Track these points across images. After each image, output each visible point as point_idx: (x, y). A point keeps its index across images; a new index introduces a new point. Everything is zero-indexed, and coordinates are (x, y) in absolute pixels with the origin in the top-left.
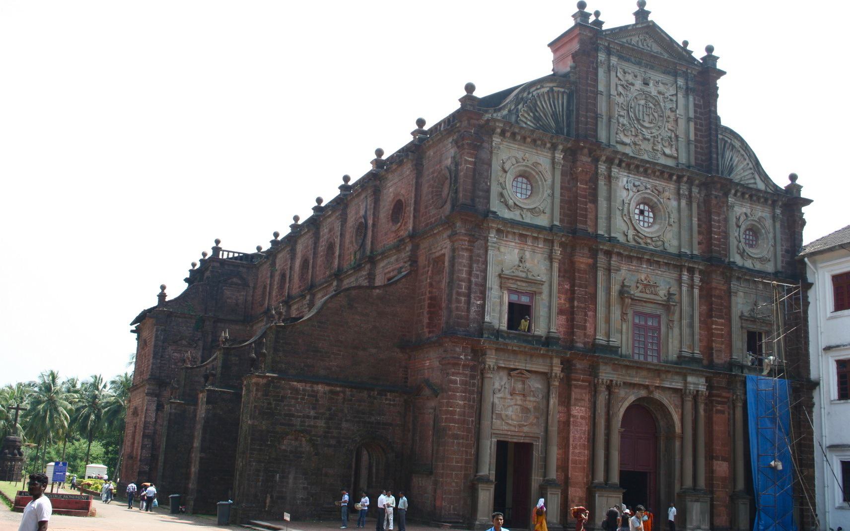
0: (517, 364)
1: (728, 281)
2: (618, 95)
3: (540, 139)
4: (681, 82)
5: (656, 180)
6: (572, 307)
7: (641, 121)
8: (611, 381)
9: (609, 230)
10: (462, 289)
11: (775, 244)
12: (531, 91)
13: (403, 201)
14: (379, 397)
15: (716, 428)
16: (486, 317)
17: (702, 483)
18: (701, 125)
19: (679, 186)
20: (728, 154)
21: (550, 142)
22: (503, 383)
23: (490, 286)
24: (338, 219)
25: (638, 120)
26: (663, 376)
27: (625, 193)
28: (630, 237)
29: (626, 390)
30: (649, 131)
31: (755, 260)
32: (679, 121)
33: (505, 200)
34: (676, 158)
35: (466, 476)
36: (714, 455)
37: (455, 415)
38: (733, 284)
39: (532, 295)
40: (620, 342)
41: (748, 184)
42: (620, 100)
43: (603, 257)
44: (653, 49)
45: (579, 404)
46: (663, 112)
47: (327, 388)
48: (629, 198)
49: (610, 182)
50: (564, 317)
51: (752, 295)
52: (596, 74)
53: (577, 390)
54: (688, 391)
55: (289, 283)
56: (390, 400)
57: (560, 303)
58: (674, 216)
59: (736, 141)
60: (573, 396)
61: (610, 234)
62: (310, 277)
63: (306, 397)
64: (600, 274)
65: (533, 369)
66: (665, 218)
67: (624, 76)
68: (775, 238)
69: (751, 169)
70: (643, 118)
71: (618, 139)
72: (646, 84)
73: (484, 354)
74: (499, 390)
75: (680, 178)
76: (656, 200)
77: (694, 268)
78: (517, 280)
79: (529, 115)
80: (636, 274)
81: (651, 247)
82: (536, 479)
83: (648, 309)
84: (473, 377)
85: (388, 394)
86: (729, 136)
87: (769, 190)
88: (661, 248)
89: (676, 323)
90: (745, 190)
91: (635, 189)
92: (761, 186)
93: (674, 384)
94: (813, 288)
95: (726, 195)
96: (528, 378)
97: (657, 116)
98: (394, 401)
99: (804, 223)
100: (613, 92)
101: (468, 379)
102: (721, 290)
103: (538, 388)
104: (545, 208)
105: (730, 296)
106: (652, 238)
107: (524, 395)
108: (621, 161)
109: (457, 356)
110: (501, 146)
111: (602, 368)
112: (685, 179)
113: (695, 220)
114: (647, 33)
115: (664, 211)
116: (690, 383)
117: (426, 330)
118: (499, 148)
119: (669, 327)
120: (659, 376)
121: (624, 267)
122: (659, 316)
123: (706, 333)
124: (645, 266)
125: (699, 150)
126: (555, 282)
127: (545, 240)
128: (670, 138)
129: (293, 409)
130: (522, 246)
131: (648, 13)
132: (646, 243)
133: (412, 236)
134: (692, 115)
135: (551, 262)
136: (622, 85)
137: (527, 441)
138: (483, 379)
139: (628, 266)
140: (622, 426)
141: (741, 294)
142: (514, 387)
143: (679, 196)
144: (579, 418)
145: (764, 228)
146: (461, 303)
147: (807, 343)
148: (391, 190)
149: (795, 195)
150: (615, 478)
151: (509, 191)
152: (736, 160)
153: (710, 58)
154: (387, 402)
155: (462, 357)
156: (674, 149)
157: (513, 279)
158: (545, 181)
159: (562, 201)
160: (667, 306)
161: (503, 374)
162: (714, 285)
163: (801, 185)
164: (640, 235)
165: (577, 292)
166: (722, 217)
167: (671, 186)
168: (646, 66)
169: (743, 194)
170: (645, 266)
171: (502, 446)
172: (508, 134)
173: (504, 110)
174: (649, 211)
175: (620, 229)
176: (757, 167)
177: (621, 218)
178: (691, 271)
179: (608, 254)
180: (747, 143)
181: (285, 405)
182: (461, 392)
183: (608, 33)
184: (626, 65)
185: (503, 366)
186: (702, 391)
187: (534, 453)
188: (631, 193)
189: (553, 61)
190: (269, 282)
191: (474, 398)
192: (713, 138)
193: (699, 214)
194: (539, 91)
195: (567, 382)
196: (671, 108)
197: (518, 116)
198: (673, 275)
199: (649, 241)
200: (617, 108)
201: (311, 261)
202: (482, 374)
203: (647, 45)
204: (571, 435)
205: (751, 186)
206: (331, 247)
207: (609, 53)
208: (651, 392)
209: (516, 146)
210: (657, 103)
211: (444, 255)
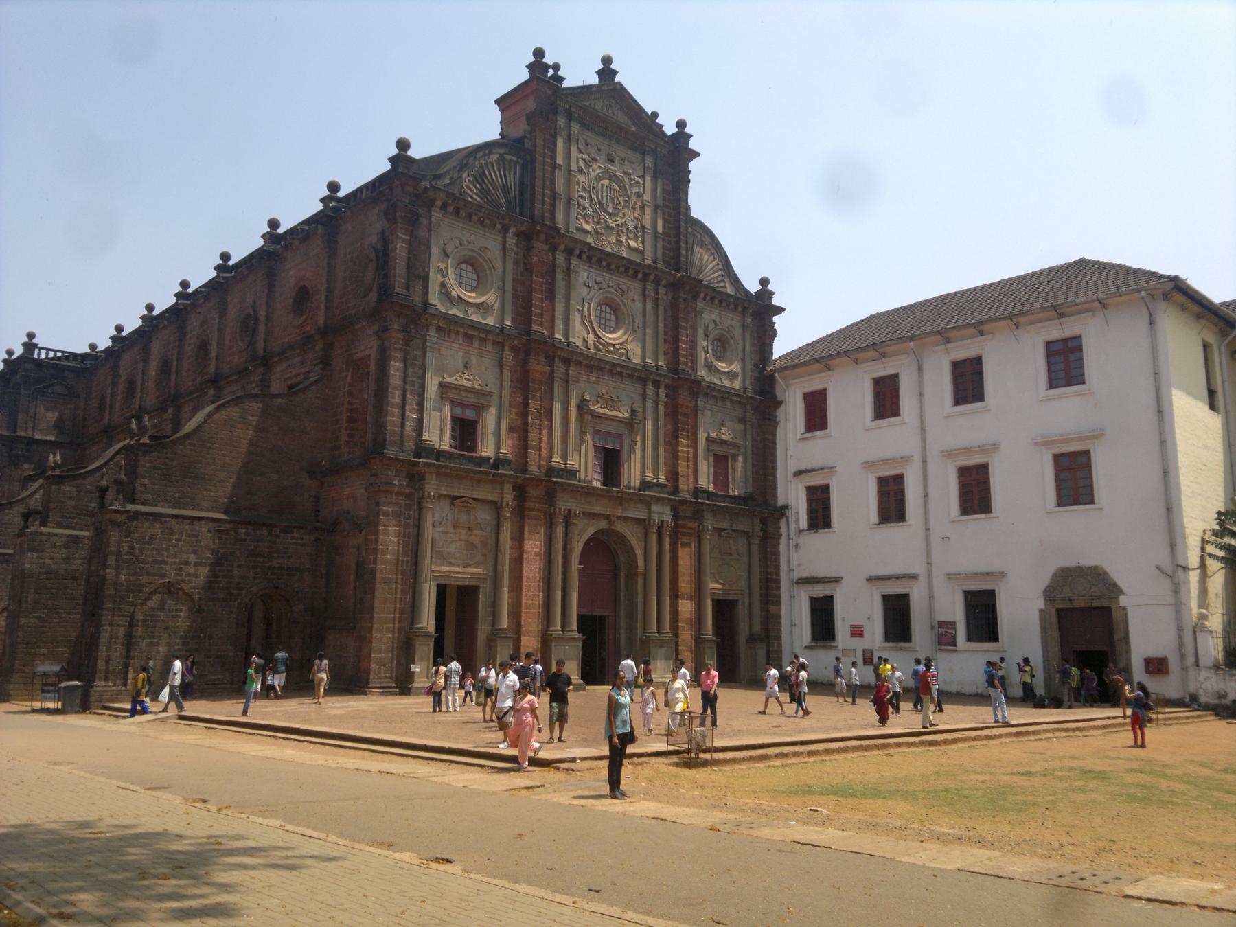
1: (695, 396)
4: (649, 162)
6: (526, 423)
7: (604, 206)
8: (570, 510)
9: (567, 334)
10: (394, 398)
12: (478, 155)
13: (309, 287)
14: (282, 534)
15: (681, 562)
16: (424, 434)
18: (670, 215)
19: (645, 285)
20: (698, 252)
22: (444, 514)
23: (429, 396)
24: (215, 309)
25: (601, 204)
27: (585, 288)
28: (590, 343)
33: (447, 291)
34: (642, 253)
35: (400, 629)
39: (480, 408)
40: (578, 464)
41: (718, 287)
43: (560, 365)
46: (628, 197)
47: (212, 525)
48: (590, 296)
49: (569, 276)
52: (555, 145)
54: (652, 521)
55: (141, 391)
56: (297, 539)
58: (639, 319)
61: (567, 338)
62: (173, 384)
63: (184, 537)
65: (480, 497)
67: (586, 149)
68: (744, 349)
69: (720, 270)
72: (611, 160)
73: (422, 478)
74: (440, 523)
75: (646, 276)
76: (619, 301)
77: (659, 381)
78: (461, 390)
79: (475, 187)
82: (482, 630)
83: (609, 427)
84: (408, 507)
85: (295, 531)
88: (624, 358)
89: (639, 444)
91: (596, 286)
92: (730, 290)
94: (783, 405)
95: (695, 298)
96: (473, 508)
97: (622, 201)
98: (302, 539)
99: (775, 334)
100: (574, 167)
101: (403, 510)
105: (696, 415)
107: (469, 529)
108: (581, 252)
110: (441, 223)
111: (559, 496)
112: (652, 278)
113: (661, 325)
116: (654, 513)
117: (344, 450)
118: (440, 225)
119: (632, 449)
122: (620, 436)
124: (606, 378)
125: (666, 244)
127: (495, 342)
129: (166, 554)
131: (615, 73)
132: (608, 352)
133: (324, 332)
134: (660, 202)
136: (584, 160)
137: (473, 583)
138: (420, 509)
140: (580, 564)
141: (708, 413)
143: (644, 295)
144: (533, 553)
146: (393, 416)
147: (774, 468)
148: (291, 273)
149: (766, 303)
150: (574, 625)
151: (451, 281)
152: (706, 258)
153: (682, 135)
154: (294, 541)
155: (396, 482)
156: (639, 242)
158: (495, 270)
159: (515, 296)
161: (445, 504)
162: (680, 401)
163: (773, 290)
165: (531, 406)
166: (690, 324)
169: (712, 299)
170: (606, 378)
171: (442, 590)
172: (450, 209)
174: (611, 314)
175: (580, 335)
177: (580, 320)
178: (656, 384)
179: (567, 361)
180: (717, 240)
181: (154, 549)
182: (394, 526)
183: (568, 91)
184: (588, 135)
185: (445, 493)
186: (668, 522)
187: (481, 596)
188: (592, 292)
189: (501, 122)
190: (109, 391)
191: (409, 533)
192: (682, 230)
193: (665, 320)
195: (520, 512)
196: (637, 193)
198: (639, 389)
200: (577, 187)
201: (175, 363)
202: (420, 503)
203: (613, 113)
204: (525, 574)
205: (720, 290)
206: (204, 346)
207: (570, 117)
208: (611, 523)
209: (461, 225)
210: (623, 187)
211: (369, 356)
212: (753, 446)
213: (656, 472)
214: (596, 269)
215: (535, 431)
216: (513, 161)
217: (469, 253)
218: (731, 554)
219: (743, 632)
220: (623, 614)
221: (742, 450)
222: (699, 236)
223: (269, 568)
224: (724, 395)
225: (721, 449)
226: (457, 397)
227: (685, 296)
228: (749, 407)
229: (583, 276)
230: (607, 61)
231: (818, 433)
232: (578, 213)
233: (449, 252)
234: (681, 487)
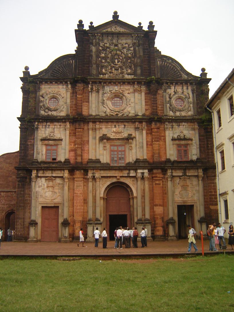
14: (15, 194)
15: (155, 191)
17: (147, 216)
21: (64, 82)
53: (76, 182)
54: (137, 176)
60: (75, 185)
64: (91, 132)
74: (41, 186)
75: (134, 83)
81: (119, 115)
87: (189, 78)
91: (110, 92)
96: (55, 180)
99: (209, 90)
106: (119, 112)
112: (136, 83)
114: (116, 25)
116: (138, 173)
120: (122, 171)
121: (104, 127)
142: (47, 185)
144: (79, 193)
195: (72, 179)
199: (118, 113)
204: (75, 202)
219: (197, 217)
221: (194, 141)
223: (11, 204)
224: (179, 121)
230: (116, 13)
231: (221, 128)
233: (44, 96)
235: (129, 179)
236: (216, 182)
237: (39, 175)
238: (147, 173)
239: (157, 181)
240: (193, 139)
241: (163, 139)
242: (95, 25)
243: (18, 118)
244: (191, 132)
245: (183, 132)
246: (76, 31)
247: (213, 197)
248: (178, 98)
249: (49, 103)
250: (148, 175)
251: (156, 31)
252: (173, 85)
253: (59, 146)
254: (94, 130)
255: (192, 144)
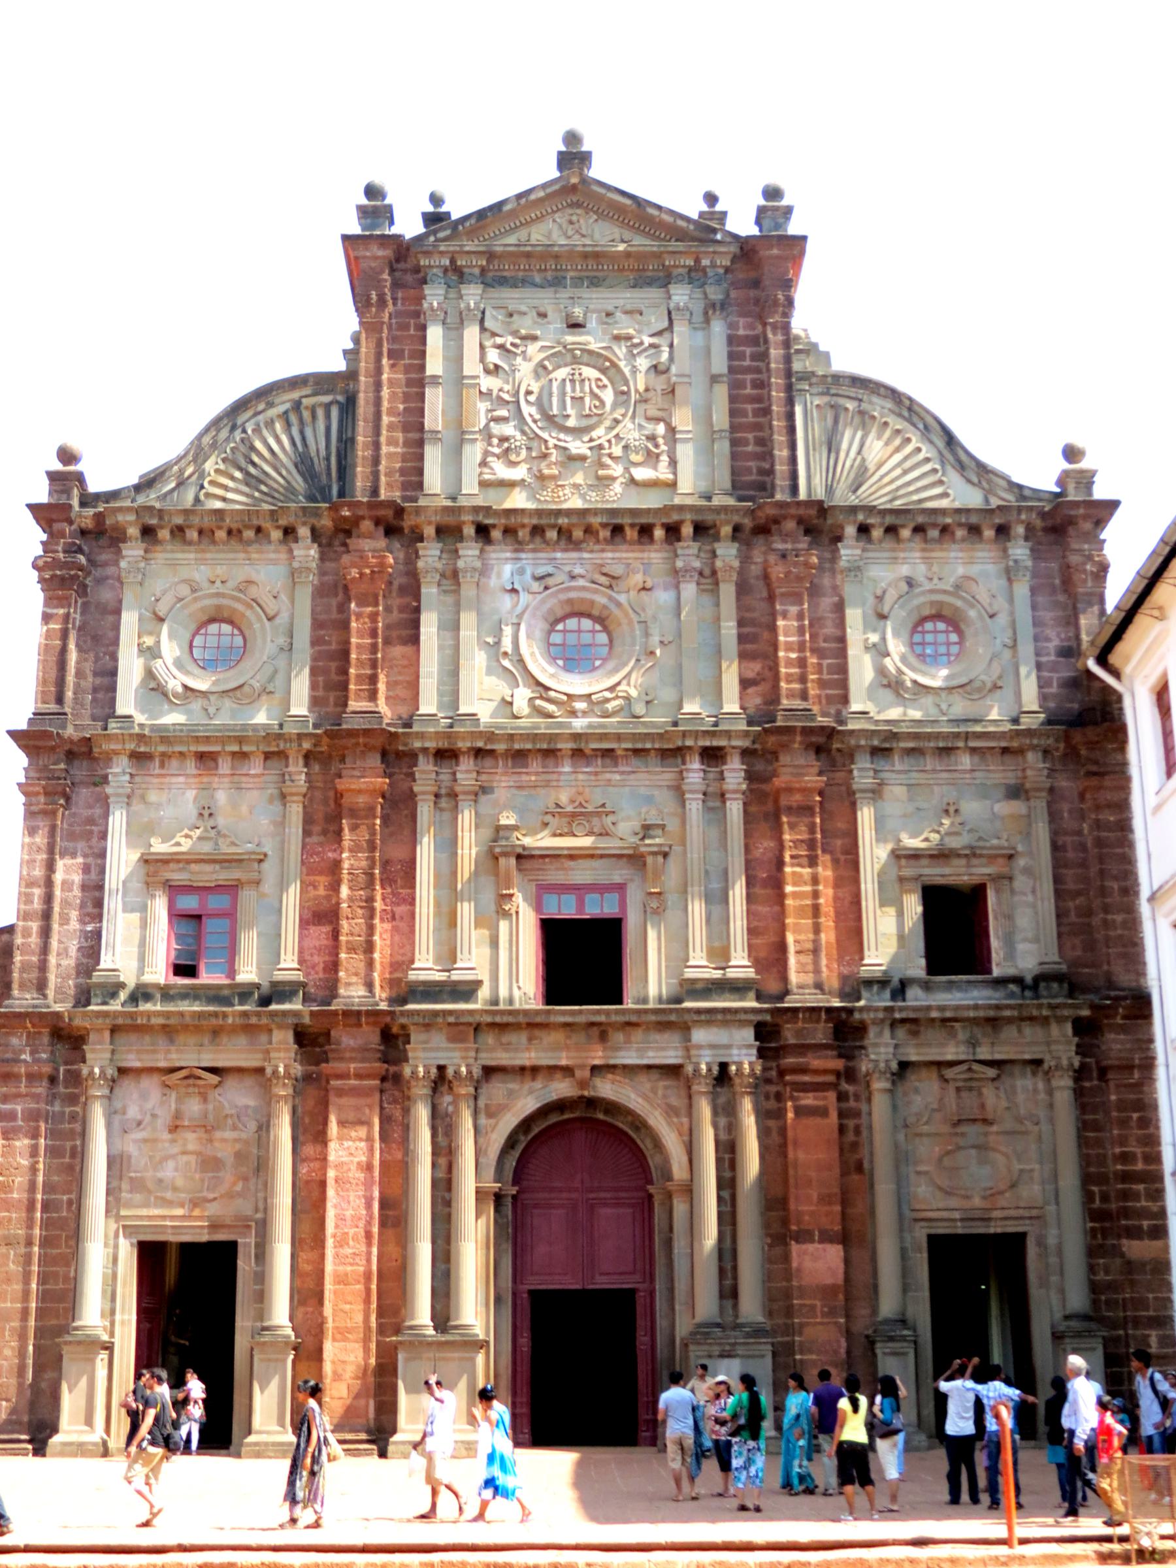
0: (174, 1056)
2: (487, 371)
3: (248, 527)
4: (681, 295)
5: (603, 551)
8: (441, 1069)
11: (1015, 641)
12: (239, 421)
15: (798, 1155)
17: (751, 1307)
21: (278, 527)
22: (149, 1105)
23: (114, 886)
25: (550, 419)
26: (618, 1037)
27: (507, 601)
29: (511, 1086)
30: (586, 439)
31: (943, 694)
32: (679, 391)
36: (794, 1228)
37: (11, 1192)
38: (861, 770)
39: (232, 889)
41: (921, 501)
42: (488, 383)
43: (431, 767)
44: (597, 236)
45: (353, 1134)
46: (626, 383)
48: (519, 609)
49: (458, 584)
50: (326, 929)
51: (936, 788)
52: (424, 343)
53: (344, 1101)
54: (689, 1069)
57: (316, 898)
59: (875, 399)
66: (633, 638)
68: (1013, 625)
70: (565, 408)
71: (486, 477)
74: (139, 1123)
78: (188, 862)
79: (233, 478)
80: (542, 791)
83: (582, 874)
86: (852, 392)
90: (889, 520)
91: (536, 586)
93: (651, 1054)
99: (1104, 568)
100: (472, 366)
102: (804, 790)
103: (247, 1107)
104: (271, 679)
109: (9, 1055)
112: (687, 530)
113: (729, 629)
114: (578, 205)
115: (630, 622)
116: (700, 1047)
120: (603, 1037)
121: (503, 781)
122: (621, 888)
123: (777, 908)
126: (293, 848)
128: (652, 438)
130: (205, 780)
132: (573, 713)
135: (285, 805)
136: (501, 347)
139: (515, 777)
141: (899, 791)
142: (178, 1115)
143: (676, 572)
144: (353, 1167)
145: (972, 606)
146: (30, 935)
147: (1129, 889)
157: (179, 861)
160: (635, 859)
161: (150, 1084)
164: (552, 694)
165: (346, 865)
166: (827, 602)
167: (653, 555)
168: (578, 282)
169: (891, 530)
172: (164, 534)
173: (167, 481)
174: (593, 631)
176: (955, 454)
178: (713, 756)
180: (910, 399)
184: (512, 297)
187: (240, 1263)
191: (74, 1148)
194: (261, 417)
196: (655, 367)
197: (202, 487)
198: (665, 775)
199: (580, 705)
209: (192, 556)
212: (1055, 847)
213: (720, 954)
214: (534, 551)
215: (360, 911)
216: (321, 405)
217: (215, 601)
218: (985, 1121)
220: (660, 1286)
221: (1021, 862)
222: (851, 405)
225: (947, 871)
226: (179, 876)
227: (779, 546)
228: (1030, 756)
229: (499, 575)
232: (486, 453)
233: (161, 614)
234: (794, 978)
235: (645, 1082)
236: (1156, 1100)
237: (133, 1062)
238: (750, 1046)
239: (811, 1095)
240: (1020, 848)
241: (846, 852)
242: (457, 208)
243: (14, 735)
244: (1005, 808)
245: (956, 811)
246: (348, 240)
247: (1141, 1187)
248: (927, 612)
249: (191, 646)
250: (754, 1059)
251: (800, 241)
252: (898, 540)
253: (247, 896)
254: (444, 803)
255: (1011, 879)
